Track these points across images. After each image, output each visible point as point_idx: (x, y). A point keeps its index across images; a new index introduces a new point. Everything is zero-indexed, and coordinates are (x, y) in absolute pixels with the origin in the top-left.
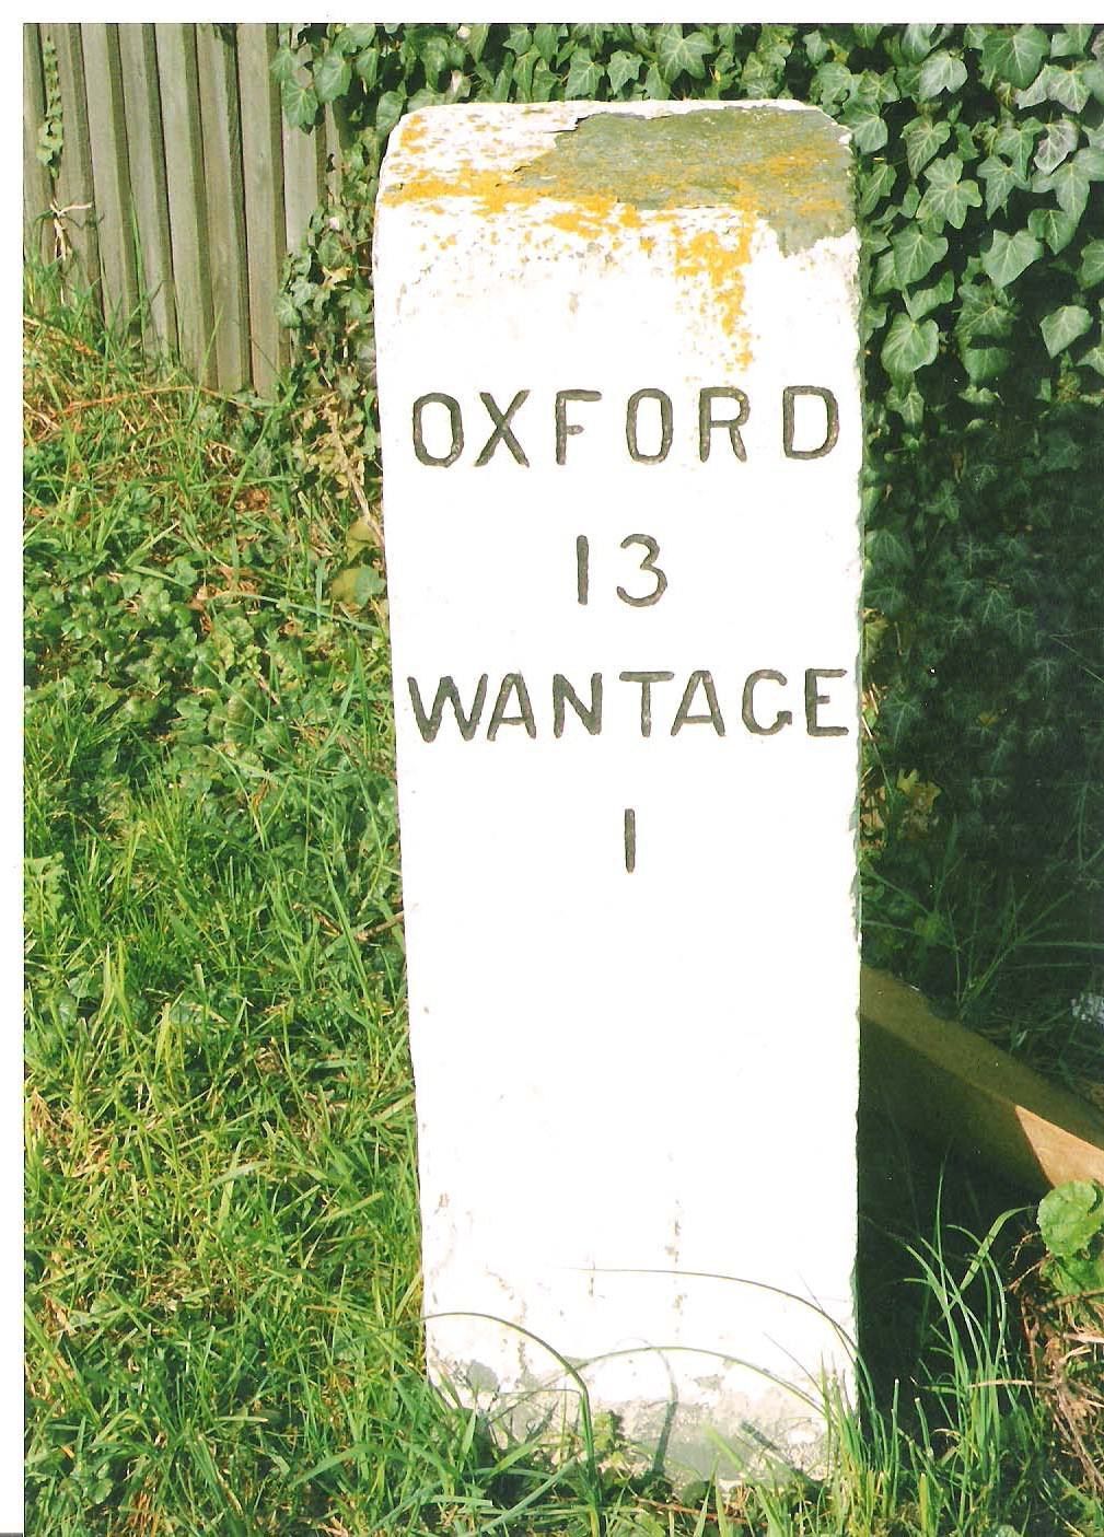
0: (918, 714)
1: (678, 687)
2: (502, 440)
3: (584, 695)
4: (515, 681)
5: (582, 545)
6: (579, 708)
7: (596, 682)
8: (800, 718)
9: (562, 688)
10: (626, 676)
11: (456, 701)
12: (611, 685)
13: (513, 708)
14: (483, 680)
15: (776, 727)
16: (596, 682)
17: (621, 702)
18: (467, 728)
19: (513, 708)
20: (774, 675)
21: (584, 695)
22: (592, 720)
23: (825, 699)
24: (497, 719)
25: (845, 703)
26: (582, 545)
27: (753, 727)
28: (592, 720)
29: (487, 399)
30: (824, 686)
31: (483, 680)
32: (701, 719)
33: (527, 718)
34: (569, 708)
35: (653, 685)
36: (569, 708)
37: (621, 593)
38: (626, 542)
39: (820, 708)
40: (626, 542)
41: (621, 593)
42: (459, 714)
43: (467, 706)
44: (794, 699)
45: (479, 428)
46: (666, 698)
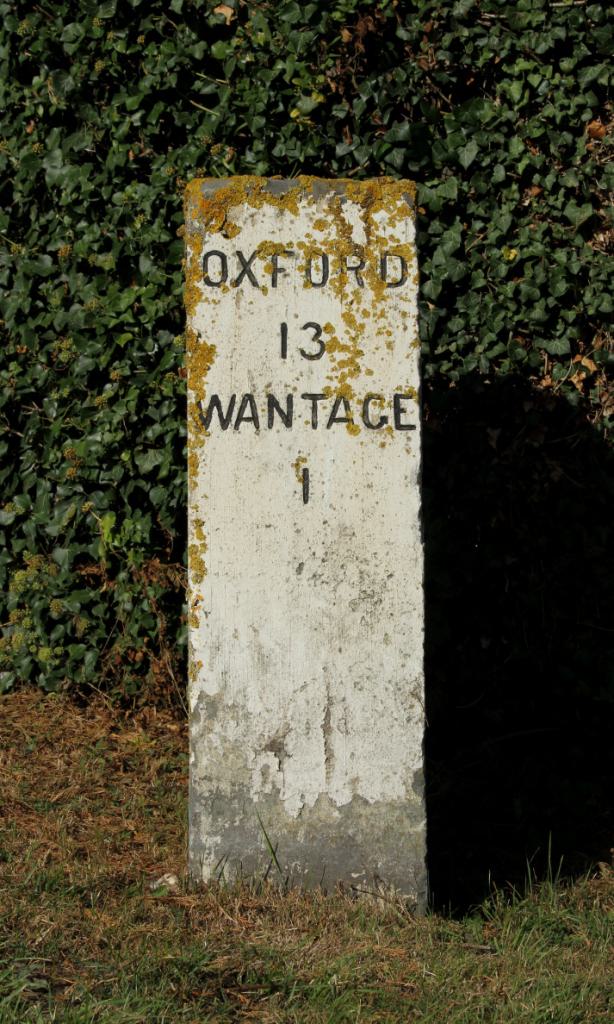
0: (174, 86)
1: (329, 403)
2: (246, 275)
3: (283, 406)
4: (249, 398)
5: (284, 328)
6: (281, 412)
7: (290, 399)
8: (391, 422)
9: (272, 402)
10: (304, 396)
11: (219, 409)
12: (297, 401)
13: (248, 413)
14: (233, 398)
15: (380, 425)
16: (290, 399)
17: (302, 408)
18: (224, 424)
19: (248, 413)
20: (379, 397)
21: (283, 406)
22: (288, 421)
23: (403, 411)
24: (240, 419)
25: (412, 412)
26: (284, 328)
27: (369, 425)
28: (288, 421)
29: (239, 254)
30: (404, 403)
31: (234, 397)
32: (341, 420)
33: (254, 419)
34: (276, 414)
35: (319, 402)
36: (276, 414)
37: (303, 353)
38: (306, 327)
39: (402, 415)
40: (306, 327)
41: (303, 353)
42: (220, 415)
43: (225, 411)
44: (389, 412)
45: (234, 271)
46: (325, 408)
